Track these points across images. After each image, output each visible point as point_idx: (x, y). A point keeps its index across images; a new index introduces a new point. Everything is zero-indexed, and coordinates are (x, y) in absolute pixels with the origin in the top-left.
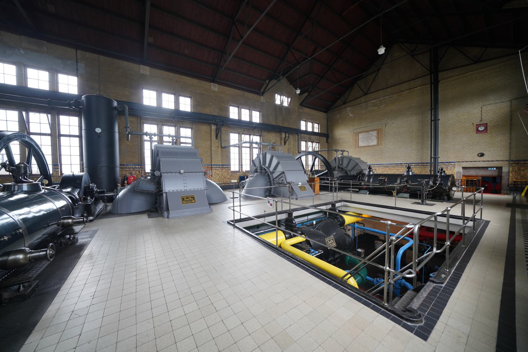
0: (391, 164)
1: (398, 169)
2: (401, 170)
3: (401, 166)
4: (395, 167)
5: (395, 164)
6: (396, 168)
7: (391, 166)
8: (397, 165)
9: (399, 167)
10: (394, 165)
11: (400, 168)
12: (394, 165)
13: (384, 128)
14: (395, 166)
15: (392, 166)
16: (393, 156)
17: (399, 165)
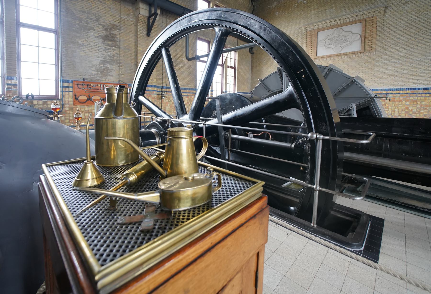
0: (396, 90)
1: (415, 101)
2: (423, 103)
3: (426, 93)
4: (408, 95)
5: (409, 89)
6: (411, 98)
7: (395, 94)
8: (414, 92)
9: (419, 95)
10: (405, 92)
11: (423, 98)
12: (405, 92)
13: (382, 14)
14: (407, 94)
15: (399, 94)
16: (403, 72)
17: (421, 91)
